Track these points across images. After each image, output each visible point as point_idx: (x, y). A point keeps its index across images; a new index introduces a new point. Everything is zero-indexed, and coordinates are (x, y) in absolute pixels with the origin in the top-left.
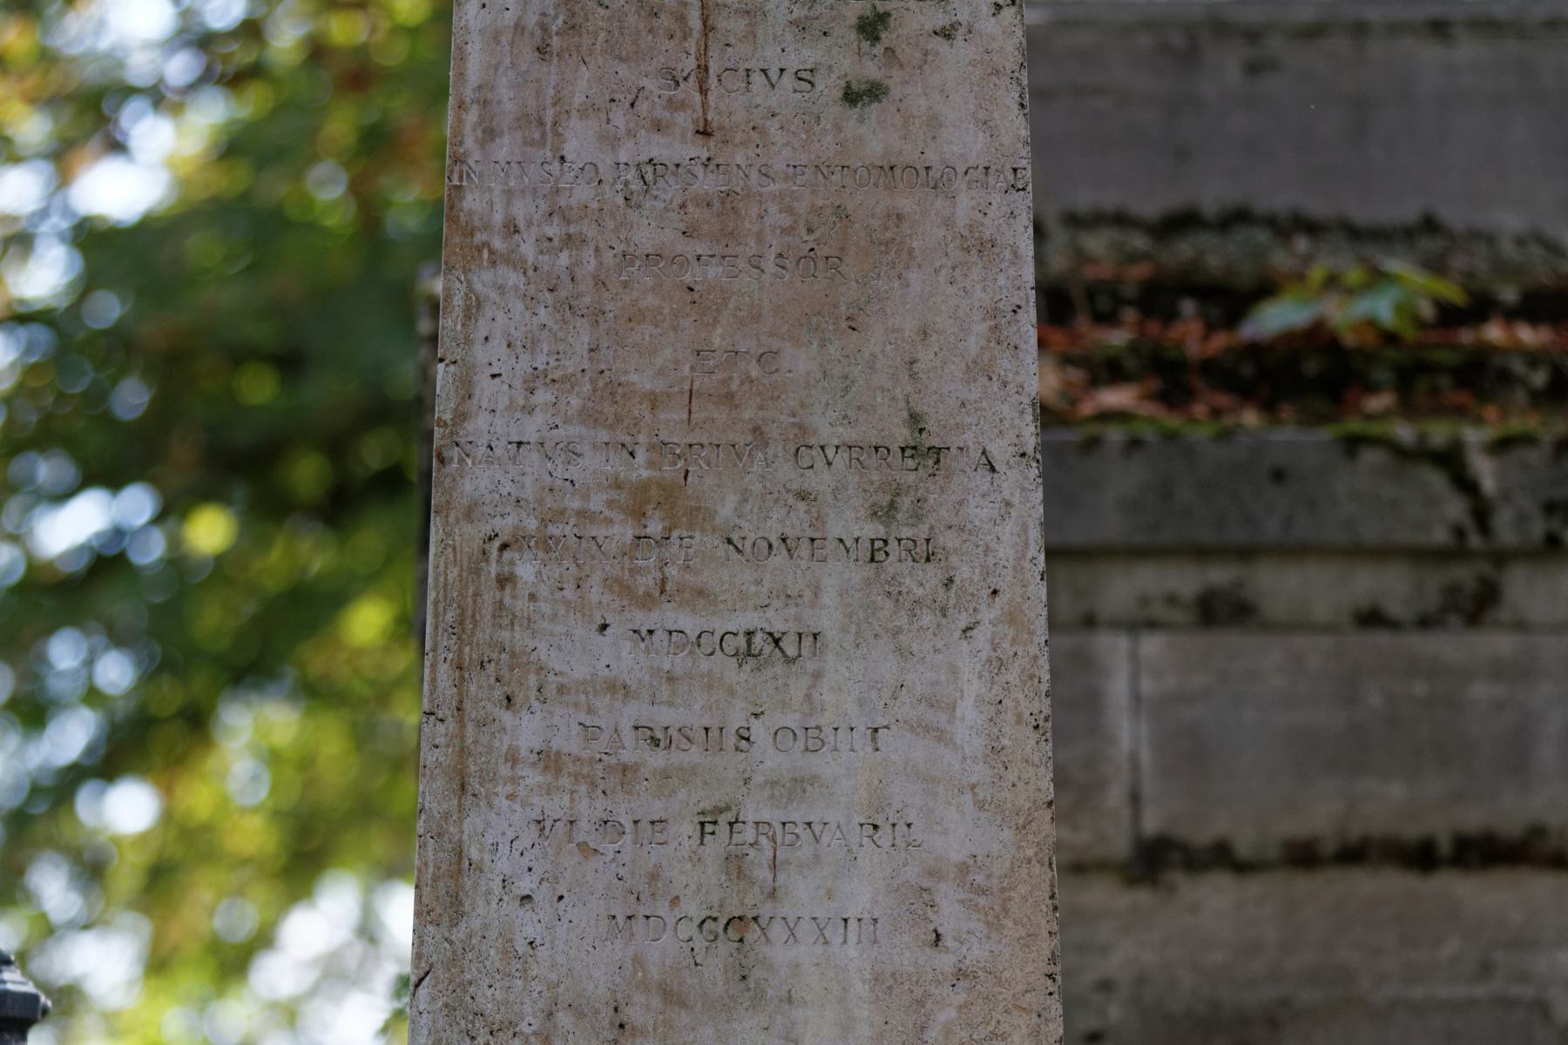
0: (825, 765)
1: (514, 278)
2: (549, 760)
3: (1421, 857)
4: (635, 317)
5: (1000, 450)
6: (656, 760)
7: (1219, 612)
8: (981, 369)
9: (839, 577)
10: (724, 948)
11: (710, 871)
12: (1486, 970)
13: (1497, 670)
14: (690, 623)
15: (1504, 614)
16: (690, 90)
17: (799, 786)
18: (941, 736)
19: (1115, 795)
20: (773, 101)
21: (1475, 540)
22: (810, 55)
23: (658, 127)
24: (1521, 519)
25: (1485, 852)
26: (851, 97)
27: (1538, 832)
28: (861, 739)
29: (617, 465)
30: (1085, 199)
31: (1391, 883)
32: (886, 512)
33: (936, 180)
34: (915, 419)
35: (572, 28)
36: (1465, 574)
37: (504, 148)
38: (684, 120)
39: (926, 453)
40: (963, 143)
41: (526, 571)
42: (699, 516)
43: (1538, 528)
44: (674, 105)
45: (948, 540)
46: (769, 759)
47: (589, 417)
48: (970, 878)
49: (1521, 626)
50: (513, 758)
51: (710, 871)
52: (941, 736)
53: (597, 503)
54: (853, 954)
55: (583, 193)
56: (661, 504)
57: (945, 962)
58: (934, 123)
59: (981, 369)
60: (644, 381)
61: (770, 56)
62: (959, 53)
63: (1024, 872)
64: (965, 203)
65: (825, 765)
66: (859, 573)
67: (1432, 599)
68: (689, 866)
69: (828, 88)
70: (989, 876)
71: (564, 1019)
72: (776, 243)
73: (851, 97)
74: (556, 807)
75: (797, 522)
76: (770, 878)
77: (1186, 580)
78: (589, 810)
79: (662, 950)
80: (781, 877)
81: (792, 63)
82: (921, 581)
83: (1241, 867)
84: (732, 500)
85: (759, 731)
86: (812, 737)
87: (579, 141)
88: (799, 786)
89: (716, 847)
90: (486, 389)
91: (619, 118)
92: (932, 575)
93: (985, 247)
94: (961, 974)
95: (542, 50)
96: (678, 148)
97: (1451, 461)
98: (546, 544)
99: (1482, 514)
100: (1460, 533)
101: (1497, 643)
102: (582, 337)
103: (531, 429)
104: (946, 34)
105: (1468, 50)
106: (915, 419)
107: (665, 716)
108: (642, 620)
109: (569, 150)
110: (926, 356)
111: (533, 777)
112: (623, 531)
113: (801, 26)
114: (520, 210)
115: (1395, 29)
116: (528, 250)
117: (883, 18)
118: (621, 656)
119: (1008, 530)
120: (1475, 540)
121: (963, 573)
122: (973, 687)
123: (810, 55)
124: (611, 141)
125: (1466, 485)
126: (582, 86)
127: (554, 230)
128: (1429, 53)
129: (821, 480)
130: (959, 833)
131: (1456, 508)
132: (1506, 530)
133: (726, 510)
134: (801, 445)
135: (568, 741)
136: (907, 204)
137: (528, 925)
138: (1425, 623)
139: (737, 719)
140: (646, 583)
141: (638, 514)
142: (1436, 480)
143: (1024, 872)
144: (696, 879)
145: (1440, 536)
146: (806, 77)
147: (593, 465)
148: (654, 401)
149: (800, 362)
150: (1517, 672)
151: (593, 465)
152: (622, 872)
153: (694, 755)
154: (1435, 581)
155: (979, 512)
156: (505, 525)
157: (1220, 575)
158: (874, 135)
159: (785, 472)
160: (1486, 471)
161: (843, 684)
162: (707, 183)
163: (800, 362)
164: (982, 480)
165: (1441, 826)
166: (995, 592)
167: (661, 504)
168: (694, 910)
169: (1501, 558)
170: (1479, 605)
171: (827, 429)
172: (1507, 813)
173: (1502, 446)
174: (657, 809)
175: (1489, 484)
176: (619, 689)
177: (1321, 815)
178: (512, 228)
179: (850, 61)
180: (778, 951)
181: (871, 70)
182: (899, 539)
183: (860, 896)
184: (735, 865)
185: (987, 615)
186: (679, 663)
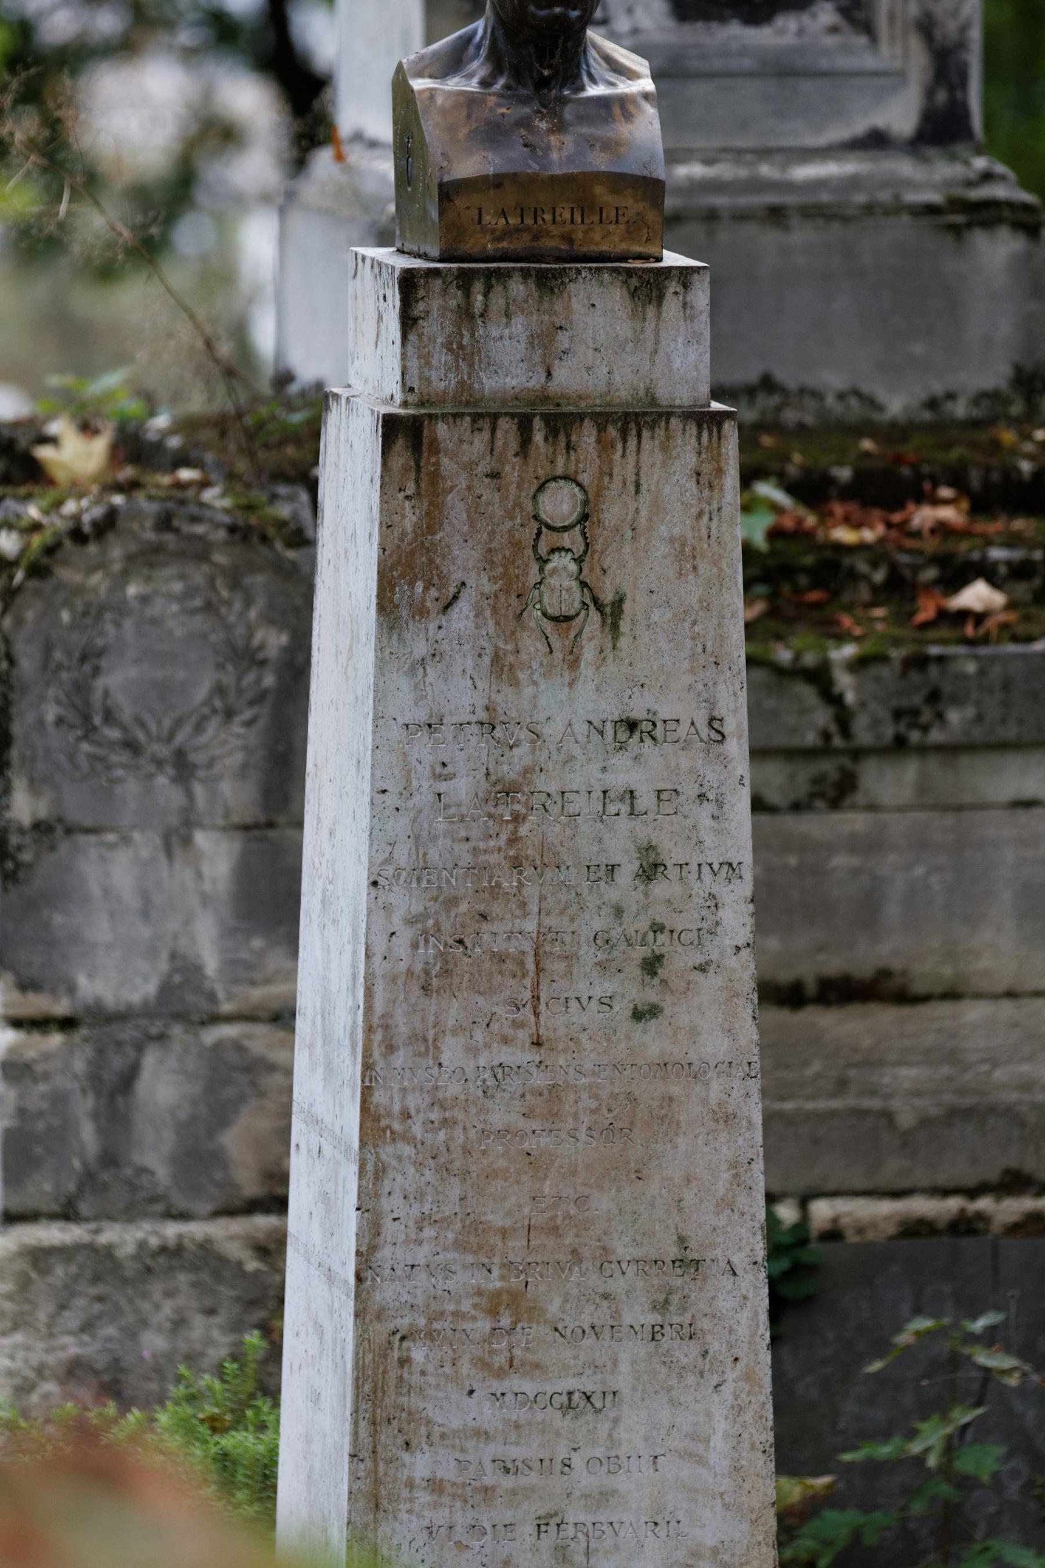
0: (622, 1482)
1: (407, 1150)
2: (435, 1486)
4: (491, 1175)
5: (740, 1260)
6: (508, 1482)
8: (726, 1204)
9: (631, 1352)
11: (544, 1557)
14: (529, 1387)
15: (860, 798)
17: (604, 1497)
18: (701, 1461)
20: (585, 1019)
21: (837, 741)
22: (608, 986)
23: (505, 1040)
24: (875, 723)
26: (638, 1015)
28: (645, 1463)
29: (478, 1279)
32: (662, 1306)
34: (682, 1241)
35: (446, 972)
36: (829, 767)
37: (400, 1058)
38: (523, 1036)
39: (689, 1264)
40: (714, 1046)
41: (418, 1354)
42: (535, 1312)
43: (888, 732)
44: (516, 1025)
45: (705, 1324)
46: (584, 1479)
47: (460, 1246)
48: (720, 1557)
49: (872, 807)
50: (410, 1485)
51: (544, 1557)
52: (701, 1461)
53: (466, 1306)
55: (453, 1089)
56: (510, 1306)
58: (694, 1032)
59: (726, 1204)
60: (496, 1219)
61: (582, 988)
62: (710, 982)
63: (756, 1552)
64: (716, 1089)
65: (622, 1482)
66: (642, 1348)
67: (802, 788)
68: (530, 1555)
69: (622, 1009)
70: (732, 1555)
72: (586, 1120)
73: (638, 1015)
74: (441, 1517)
75: (602, 1315)
76: (585, 1562)
78: (462, 1518)
80: (592, 1561)
81: (597, 992)
82: (687, 1353)
84: (557, 1301)
85: (577, 1461)
86: (612, 1463)
87: (451, 1051)
88: (604, 1497)
90: (389, 1228)
91: (479, 1035)
92: (693, 1348)
93: (727, 1118)
95: (426, 989)
96: (520, 1055)
97: (819, 677)
98: (431, 1335)
99: (844, 720)
100: (826, 736)
101: (853, 822)
102: (455, 1190)
103: (421, 1255)
104: (702, 968)
105: (802, 234)
106: (682, 1241)
107: (514, 1452)
108: (497, 1386)
109: (445, 1058)
110: (689, 1197)
111: (424, 1497)
112: (484, 1325)
113: (603, 966)
116: (417, 1130)
117: (659, 958)
118: (483, 1412)
119: (745, 1316)
120: (837, 741)
121: (716, 1346)
122: (721, 1425)
124: (473, 1051)
125: (833, 699)
126: (453, 1012)
127: (435, 1115)
128: (769, 238)
129: (618, 1286)
131: (823, 716)
132: (863, 733)
133: (553, 1308)
134: (605, 1259)
135: (448, 1472)
136: (676, 1090)
138: (797, 807)
139: (562, 1453)
140: (500, 1360)
141: (494, 1312)
142: (808, 693)
143: (756, 1552)
145: (811, 739)
146: (607, 1002)
147: (465, 1280)
148: (504, 1233)
149: (602, 1203)
150: (868, 846)
151: (465, 1280)
152: (485, 1560)
153: (532, 1478)
154: (805, 772)
155: (725, 1304)
156: (403, 1323)
158: (652, 1042)
159: (594, 1280)
160: (845, 682)
161: (633, 1427)
162: (539, 1080)
163: (602, 1203)
164: (727, 1281)
166: (736, 1359)
167: (510, 1306)
169: (858, 754)
170: (839, 792)
171: (623, 1249)
173: (859, 665)
174: (509, 1516)
175: (850, 698)
176: (481, 1434)
178: (406, 1115)
181: (652, 996)
182: (672, 1323)
185: (731, 1375)
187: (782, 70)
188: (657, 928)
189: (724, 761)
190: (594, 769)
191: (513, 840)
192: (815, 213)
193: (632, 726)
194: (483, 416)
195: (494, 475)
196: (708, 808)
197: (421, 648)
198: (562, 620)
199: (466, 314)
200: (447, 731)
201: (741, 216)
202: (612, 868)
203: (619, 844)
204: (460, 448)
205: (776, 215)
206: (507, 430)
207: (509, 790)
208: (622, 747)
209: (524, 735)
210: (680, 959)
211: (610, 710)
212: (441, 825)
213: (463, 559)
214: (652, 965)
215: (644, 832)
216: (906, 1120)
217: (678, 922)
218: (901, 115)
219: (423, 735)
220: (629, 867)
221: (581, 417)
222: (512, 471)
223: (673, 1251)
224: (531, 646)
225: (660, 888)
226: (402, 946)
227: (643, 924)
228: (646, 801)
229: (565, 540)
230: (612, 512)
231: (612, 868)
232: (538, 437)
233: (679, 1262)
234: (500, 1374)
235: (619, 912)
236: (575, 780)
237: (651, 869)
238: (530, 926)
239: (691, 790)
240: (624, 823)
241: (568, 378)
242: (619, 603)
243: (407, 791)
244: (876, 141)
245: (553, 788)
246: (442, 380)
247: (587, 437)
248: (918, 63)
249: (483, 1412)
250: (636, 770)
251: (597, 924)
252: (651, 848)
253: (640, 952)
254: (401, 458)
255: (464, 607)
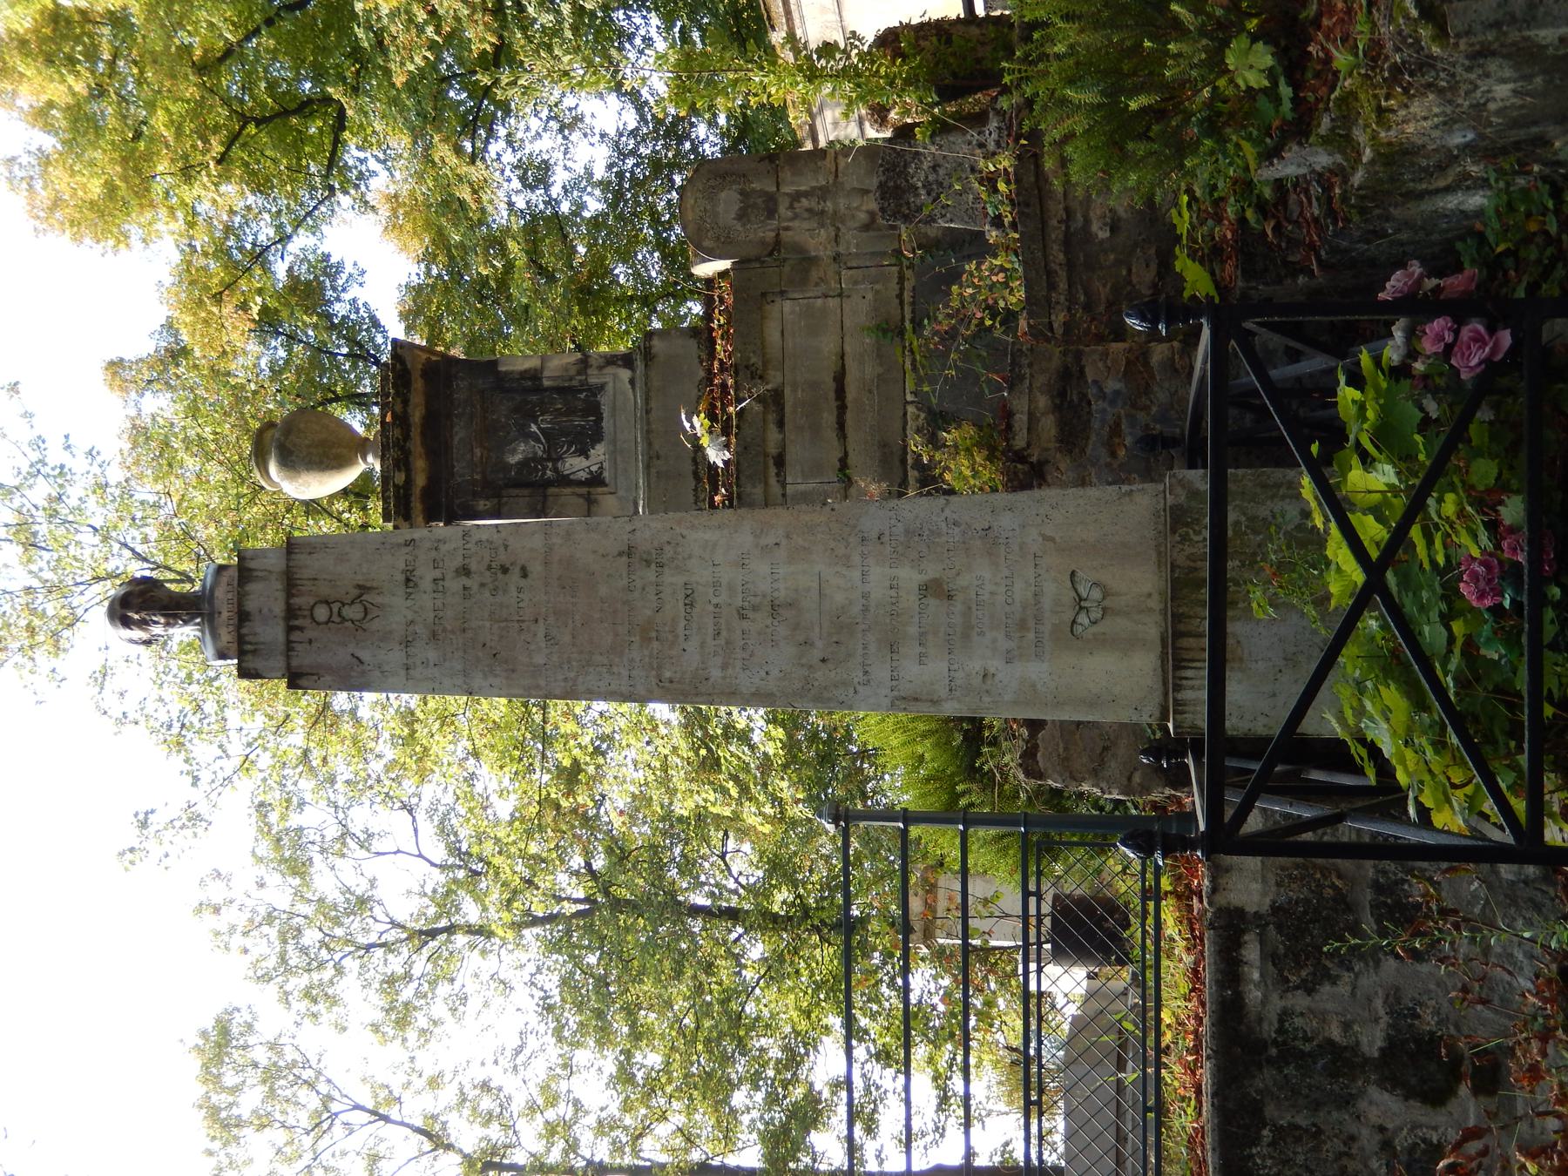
1: (580, 679)
2: (724, 667)
3: (842, 408)
5: (629, 528)
6: (724, 633)
7: (780, 462)
10: (781, 611)
12: (870, 391)
13: (794, 391)
14: (683, 623)
16: (524, 625)
19: (826, 487)
22: (513, 589)
25: (840, 392)
27: (835, 379)
28: (717, 569)
30: (692, 499)
31: (849, 416)
32: (648, 563)
33: (549, 550)
34: (620, 554)
35: (506, 662)
37: (542, 683)
39: (629, 552)
41: (668, 674)
45: (656, 543)
46: (723, 598)
50: (724, 678)
52: (715, 545)
53: (646, 652)
54: (782, 570)
55: (555, 658)
56: (648, 632)
57: (784, 542)
58: (532, 550)
66: (666, 570)
69: (523, 583)
71: (804, 661)
74: (739, 664)
75: (651, 590)
77: (773, 470)
79: (783, 631)
83: (846, 454)
85: (715, 601)
86: (716, 585)
87: (539, 659)
89: (751, 615)
90: (613, 687)
91: (533, 647)
92: (667, 548)
94: (788, 537)
96: (541, 630)
98: (660, 667)
102: (598, 658)
103: (625, 673)
104: (506, 547)
105: (653, 404)
106: (620, 554)
107: (710, 631)
108: (682, 638)
111: (730, 671)
114: (561, 677)
115: (648, 423)
116: (572, 675)
118: (692, 646)
119: (653, 525)
121: (666, 538)
123: (513, 589)
128: (653, 415)
130: (745, 539)
133: (648, 612)
135: (719, 660)
137: (775, 672)
139: (711, 608)
140: (670, 637)
141: (650, 639)
144: (761, 620)
146: (520, 590)
148: (617, 635)
149: (603, 590)
150: (795, 386)
153: (722, 621)
156: (654, 681)
157: (771, 462)
158: (536, 568)
159: (636, 594)
162: (551, 620)
163: (603, 590)
164: (638, 533)
165: (834, 404)
168: (769, 622)
172: (830, 385)
174: (739, 632)
176: (703, 645)
177: (831, 434)
179: (514, 577)
180: (782, 594)
181: (517, 570)
183: (763, 568)
184: (755, 608)
185: (678, 530)
186: (694, 625)
187: (614, 409)
188: (489, 568)
189: (421, 540)
190: (425, 597)
191: (453, 632)
192: (647, 400)
193: (408, 580)
194: (289, 646)
195: (310, 642)
196: (441, 546)
197: (377, 673)
198: (366, 612)
199: (254, 652)
200: (410, 661)
201: (648, 423)
202: (465, 588)
203: (454, 585)
204: (303, 658)
205: (648, 412)
206: (296, 636)
207: (434, 635)
208: (416, 585)
209: (411, 628)
210: (503, 557)
211: (401, 591)
212: (447, 664)
213: (342, 656)
214: (505, 570)
215: (449, 576)
216: (880, 370)
217: (487, 559)
218: (625, 374)
219: (411, 672)
220: (464, 581)
221: (288, 604)
222: (309, 634)
223: (624, 559)
224: (375, 625)
225: (473, 567)
226: (496, 682)
227: (488, 574)
228: (438, 574)
229: (335, 610)
230: (324, 590)
231: (465, 588)
232: (297, 623)
233: (629, 555)
234: (677, 636)
235: (482, 585)
236: (429, 604)
237: (465, 571)
238: (488, 624)
239: (434, 554)
240: (447, 584)
241: (279, 608)
242: (359, 587)
243: (433, 679)
244: (632, 382)
245: (432, 615)
246: (280, 662)
247: (296, 601)
248: (610, 370)
249: (692, 646)
250: (426, 576)
251: (487, 594)
252: (457, 571)
253: (500, 576)
254: (303, 682)
255: (360, 654)
